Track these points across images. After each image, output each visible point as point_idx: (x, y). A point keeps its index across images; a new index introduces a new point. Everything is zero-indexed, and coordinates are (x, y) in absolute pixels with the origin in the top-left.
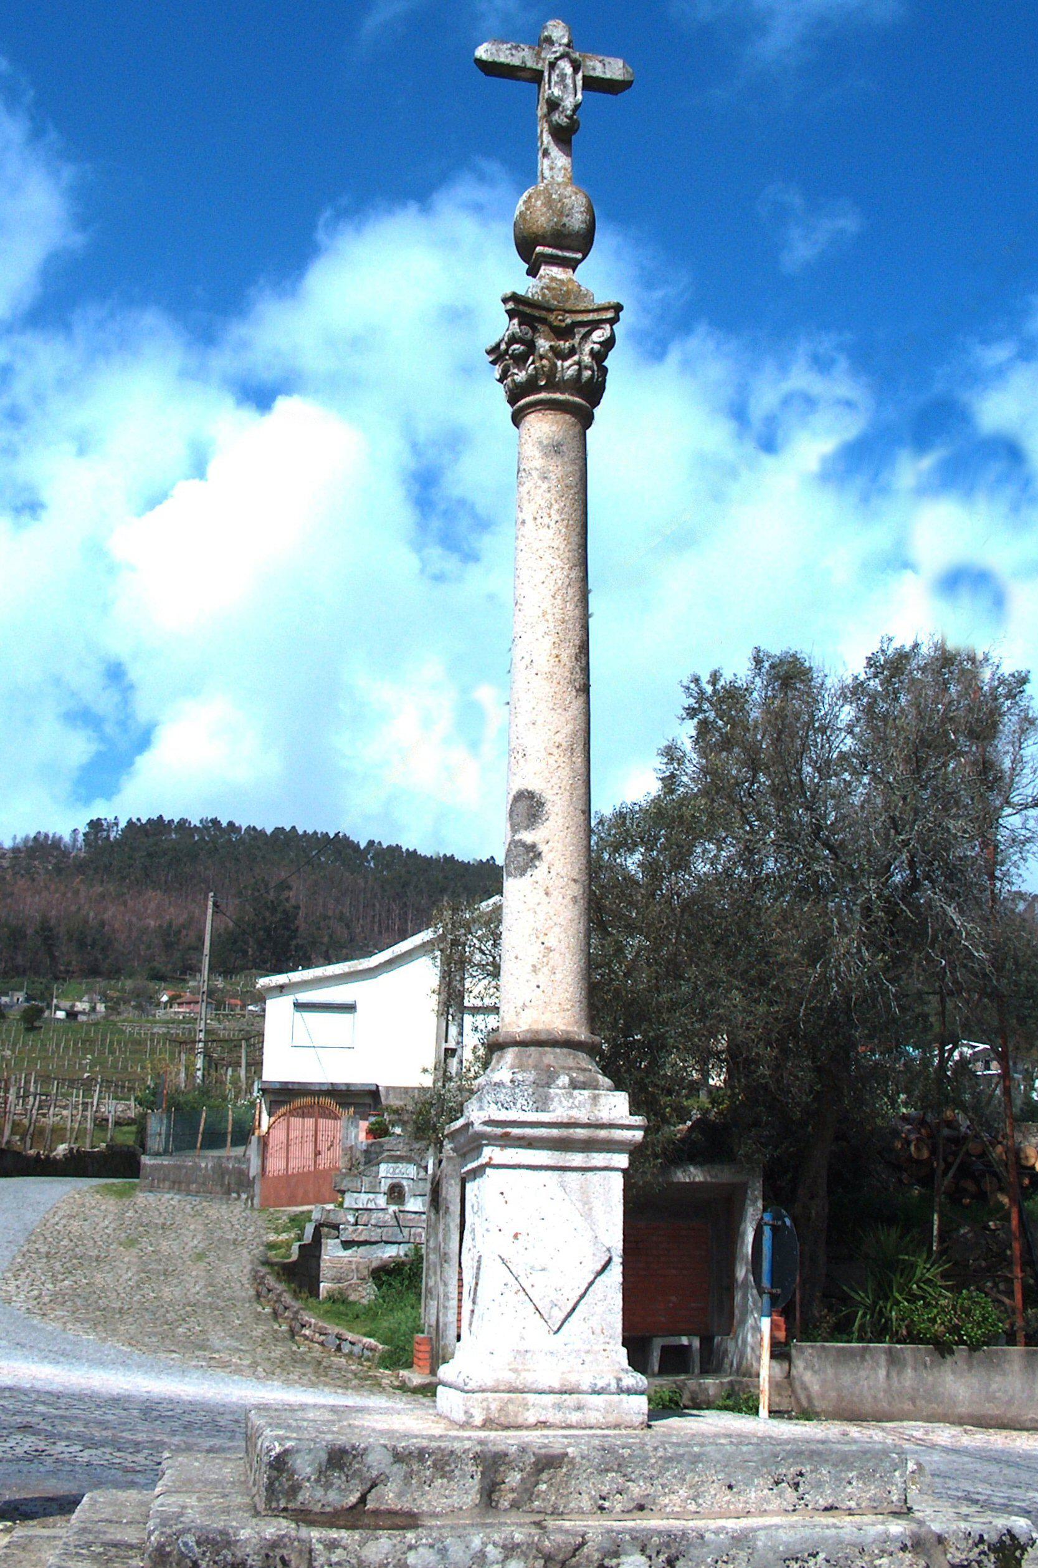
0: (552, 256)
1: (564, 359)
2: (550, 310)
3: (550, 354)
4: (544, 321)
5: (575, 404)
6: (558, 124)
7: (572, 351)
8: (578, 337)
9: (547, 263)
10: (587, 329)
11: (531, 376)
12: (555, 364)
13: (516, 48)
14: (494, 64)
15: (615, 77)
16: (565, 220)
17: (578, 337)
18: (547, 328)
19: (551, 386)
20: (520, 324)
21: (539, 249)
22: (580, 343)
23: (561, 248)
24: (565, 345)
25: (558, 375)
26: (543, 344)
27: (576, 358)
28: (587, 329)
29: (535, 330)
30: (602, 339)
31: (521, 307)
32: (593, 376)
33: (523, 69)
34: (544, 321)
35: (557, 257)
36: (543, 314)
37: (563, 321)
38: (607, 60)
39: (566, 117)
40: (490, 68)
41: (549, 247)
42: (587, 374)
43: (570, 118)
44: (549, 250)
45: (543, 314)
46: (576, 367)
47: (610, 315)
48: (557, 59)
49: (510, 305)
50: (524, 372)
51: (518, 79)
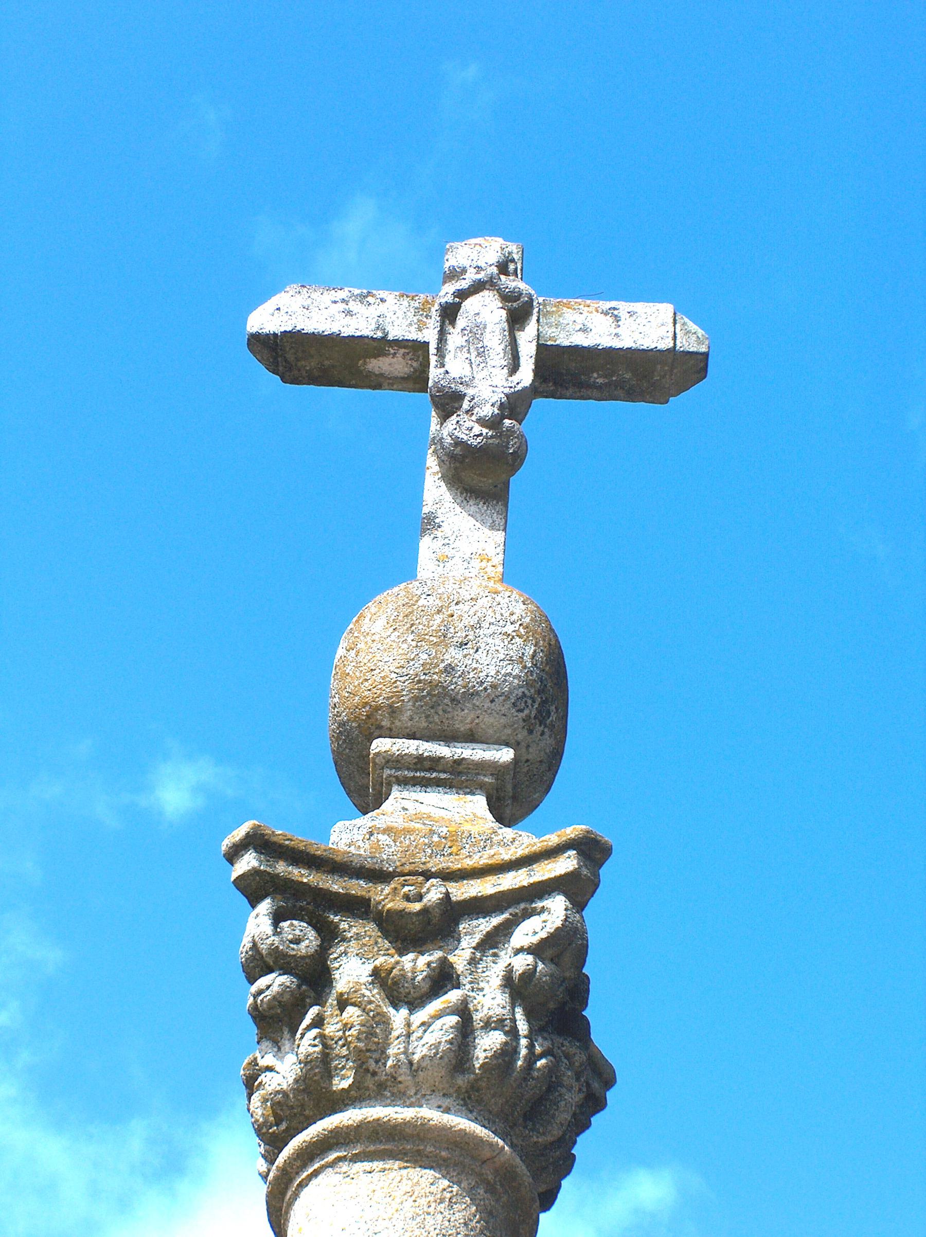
0: (420, 762)
1: (414, 1004)
2: (379, 876)
3: (374, 994)
4: (358, 907)
5: (444, 1136)
6: (458, 443)
7: (443, 978)
8: (468, 943)
9: (405, 783)
10: (496, 920)
11: (307, 1062)
12: (384, 1021)
13: (362, 298)
14: (295, 338)
15: (647, 343)
16: (453, 655)
17: (468, 943)
18: (371, 928)
19: (374, 1084)
20: (278, 918)
21: (380, 745)
22: (473, 962)
23: (449, 738)
24: (417, 964)
25: (394, 1050)
26: (351, 971)
27: (453, 996)
28: (496, 920)
29: (329, 936)
30: (535, 940)
31: (281, 868)
32: (507, 1053)
33: (381, 345)
34: (358, 907)
35: (435, 763)
36: (358, 887)
37: (420, 897)
38: (623, 307)
39: (482, 422)
40: (294, 357)
41: (412, 736)
42: (488, 1043)
43: (492, 423)
44: (412, 747)
45: (358, 887)
46: (454, 1019)
47: (566, 864)
48: (463, 295)
49: (249, 861)
50: (291, 1058)
51: (375, 382)
